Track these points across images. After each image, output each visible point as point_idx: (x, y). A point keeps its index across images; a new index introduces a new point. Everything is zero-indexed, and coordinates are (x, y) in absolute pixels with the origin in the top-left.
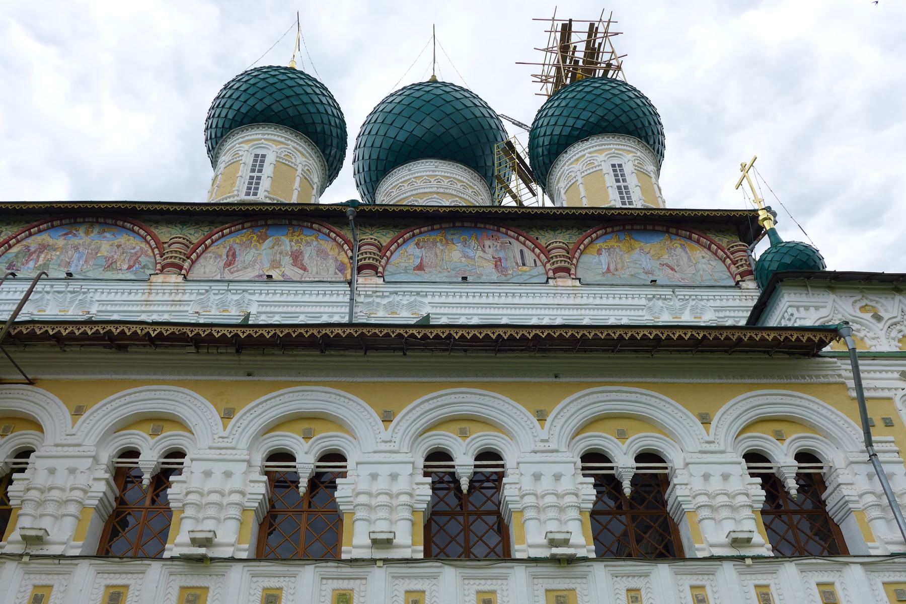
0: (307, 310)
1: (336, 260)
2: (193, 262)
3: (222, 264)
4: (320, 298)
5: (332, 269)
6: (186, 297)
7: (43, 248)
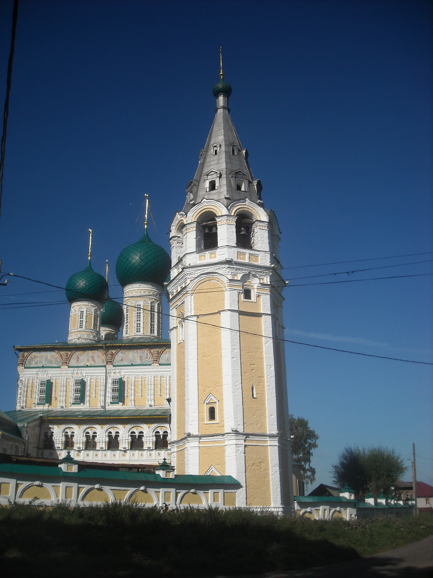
0: (96, 374)
5: (101, 362)
7: (35, 357)
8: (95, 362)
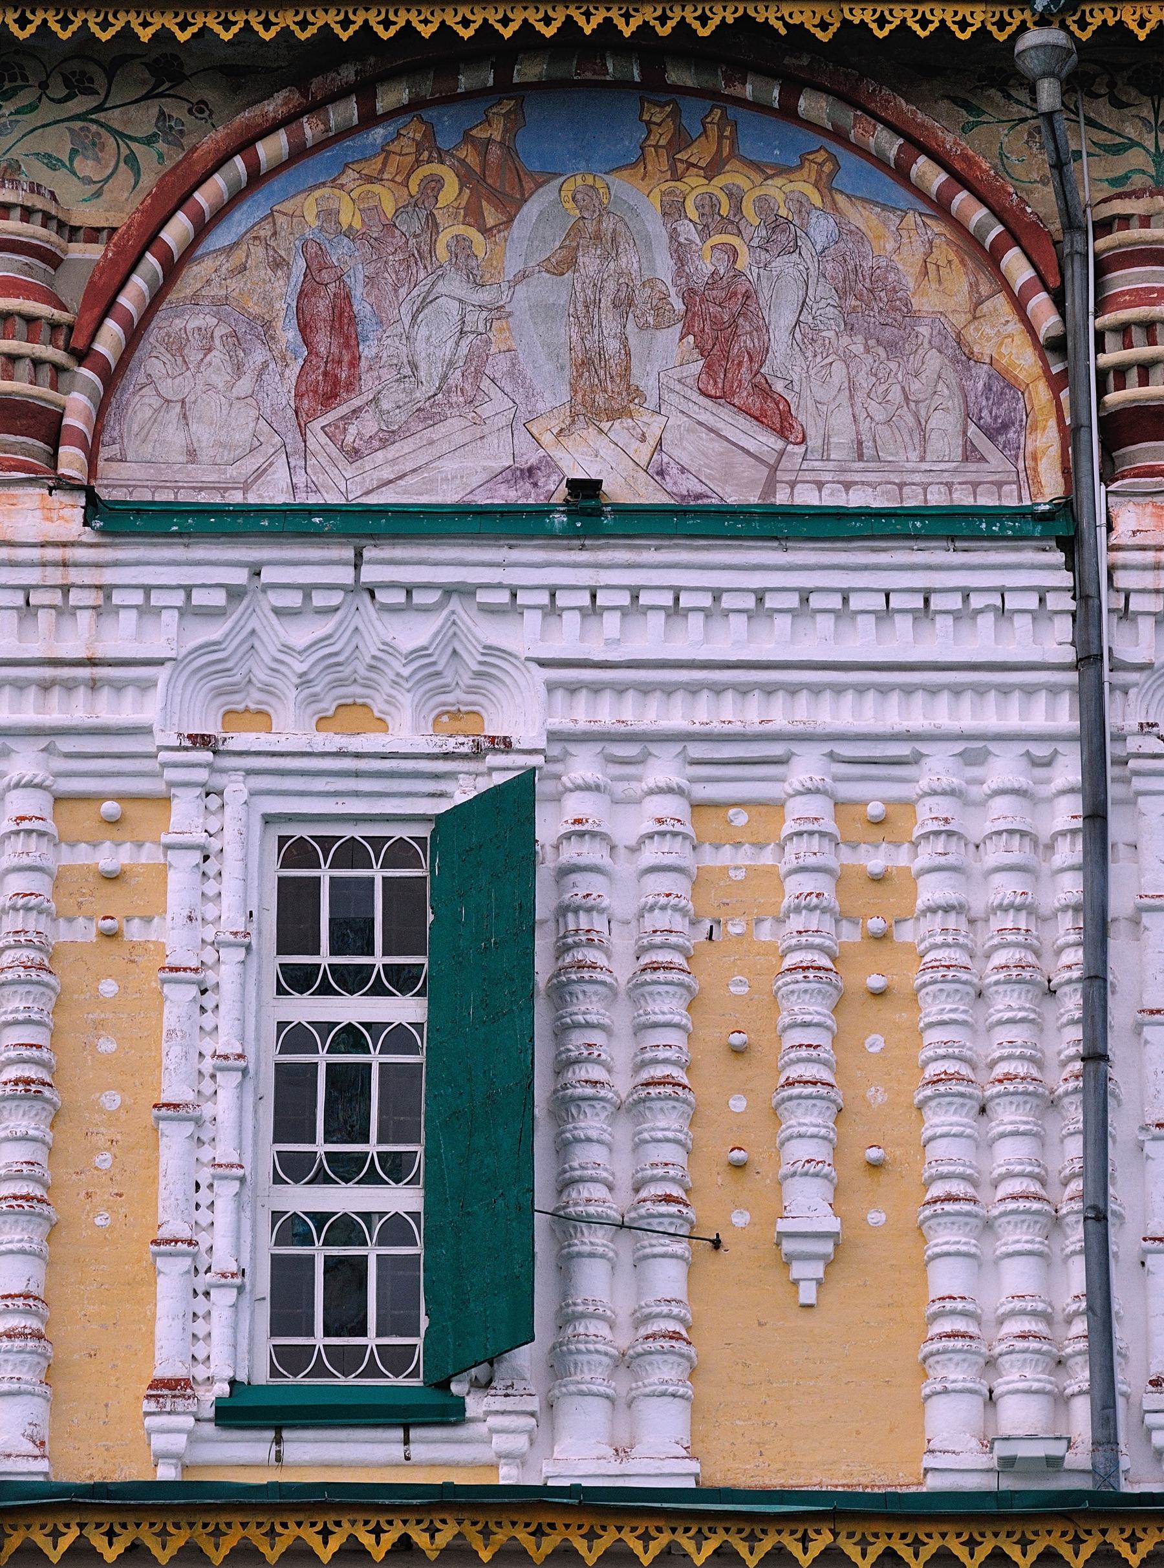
0: (833, 715)
1: (964, 355)
2: (112, 377)
3: (281, 389)
4: (902, 642)
5: (945, 424)
6: (121, 637)
8: (782, 423)
